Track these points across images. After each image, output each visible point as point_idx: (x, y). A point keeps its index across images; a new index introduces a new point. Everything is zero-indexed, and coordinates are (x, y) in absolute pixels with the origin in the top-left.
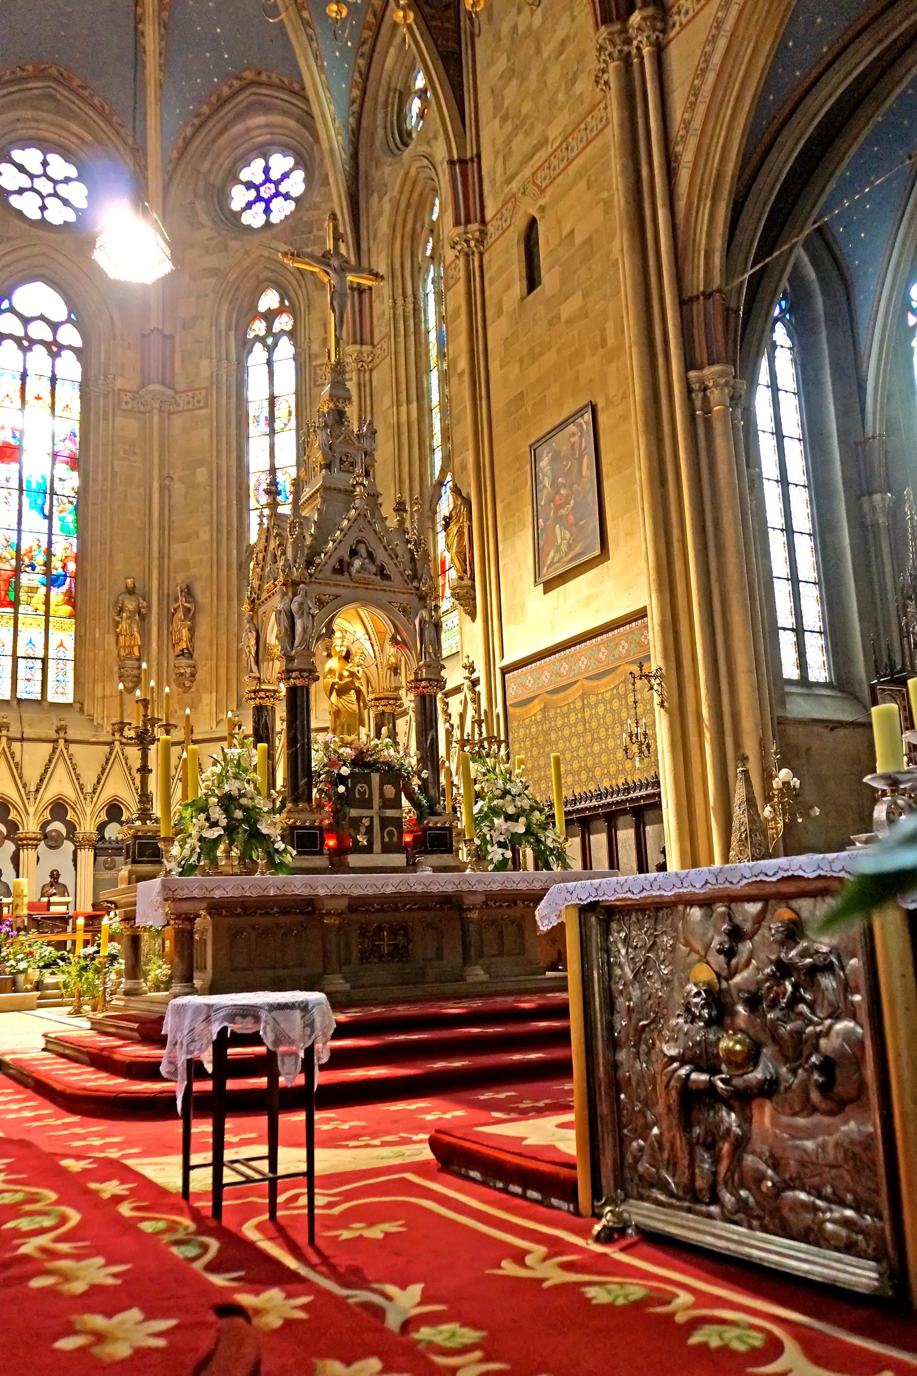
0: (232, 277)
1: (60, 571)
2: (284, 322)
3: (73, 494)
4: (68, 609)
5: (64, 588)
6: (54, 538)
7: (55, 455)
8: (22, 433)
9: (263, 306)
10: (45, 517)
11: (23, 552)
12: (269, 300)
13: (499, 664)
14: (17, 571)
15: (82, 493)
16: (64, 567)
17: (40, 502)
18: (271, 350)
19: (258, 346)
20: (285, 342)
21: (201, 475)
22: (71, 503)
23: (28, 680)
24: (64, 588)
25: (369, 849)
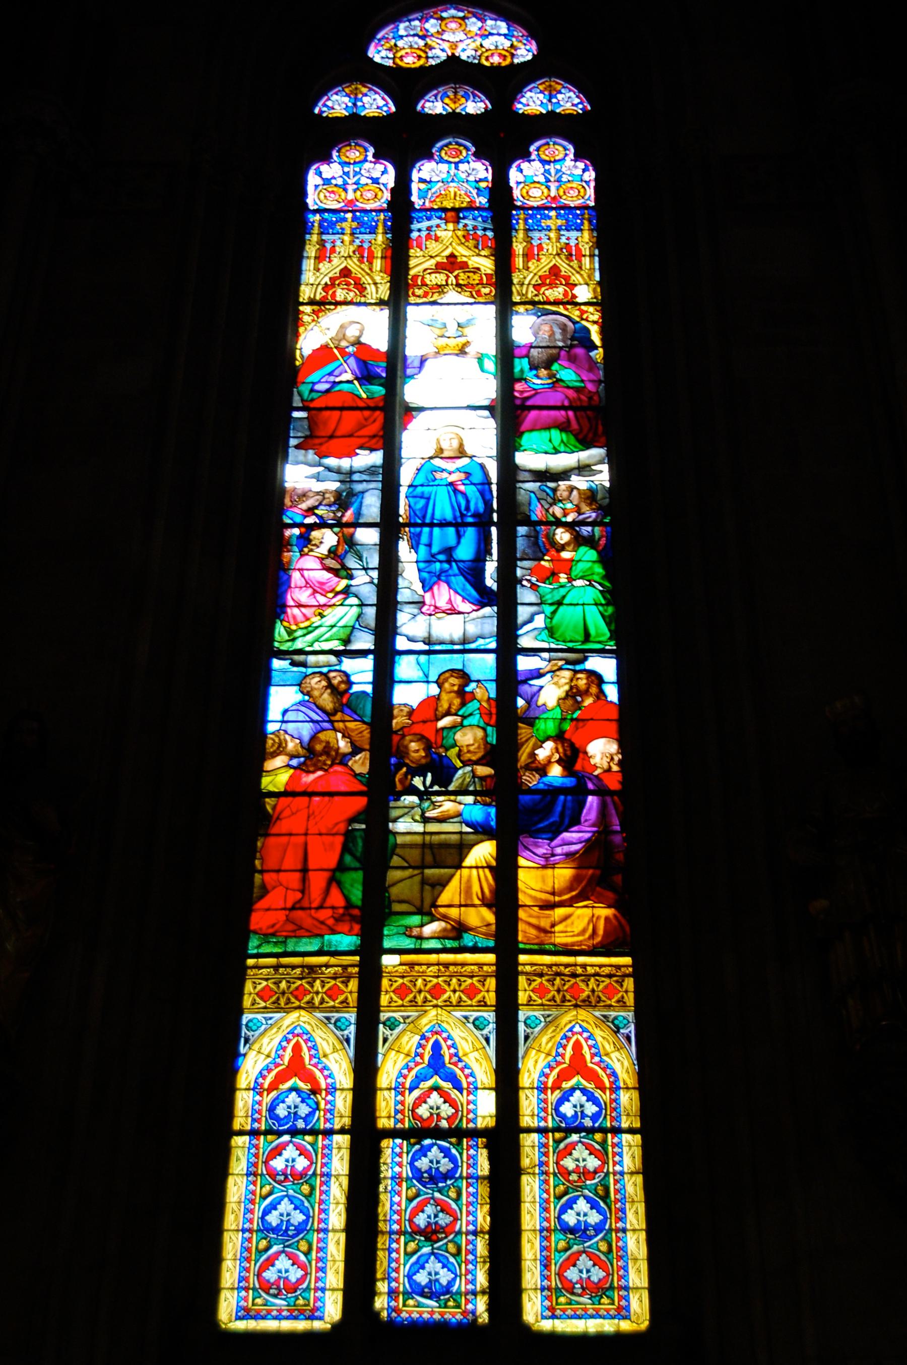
3: (590, 514)
6: (524, 663)
10: (484, 598)
11: (398, 721)
17: (465, 551)
22: (590, 542)
23: (431, 1234)
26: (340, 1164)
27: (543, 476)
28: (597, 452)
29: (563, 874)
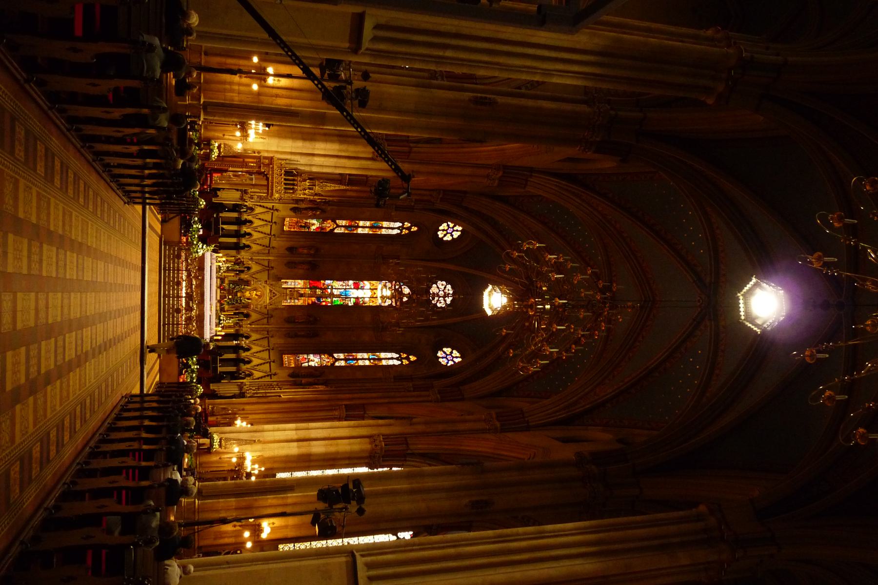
1: (322, 300)
4: (310, 302)
5: (316, 301)
7: (357, 298)
8: (364, 289)
9: (410, 357)
12: (412, 358)
13: (281, 395)
15: (347, 305)
16: (323, 302)
18: (397, 359)
19: (398, 356)
20: (400, 362)
22: (343, 303)
24: (316, 301)
25: (221, 293)
26: (292, 287)
27: (350, 300)
28: (353, 304)
29: (314, 301)
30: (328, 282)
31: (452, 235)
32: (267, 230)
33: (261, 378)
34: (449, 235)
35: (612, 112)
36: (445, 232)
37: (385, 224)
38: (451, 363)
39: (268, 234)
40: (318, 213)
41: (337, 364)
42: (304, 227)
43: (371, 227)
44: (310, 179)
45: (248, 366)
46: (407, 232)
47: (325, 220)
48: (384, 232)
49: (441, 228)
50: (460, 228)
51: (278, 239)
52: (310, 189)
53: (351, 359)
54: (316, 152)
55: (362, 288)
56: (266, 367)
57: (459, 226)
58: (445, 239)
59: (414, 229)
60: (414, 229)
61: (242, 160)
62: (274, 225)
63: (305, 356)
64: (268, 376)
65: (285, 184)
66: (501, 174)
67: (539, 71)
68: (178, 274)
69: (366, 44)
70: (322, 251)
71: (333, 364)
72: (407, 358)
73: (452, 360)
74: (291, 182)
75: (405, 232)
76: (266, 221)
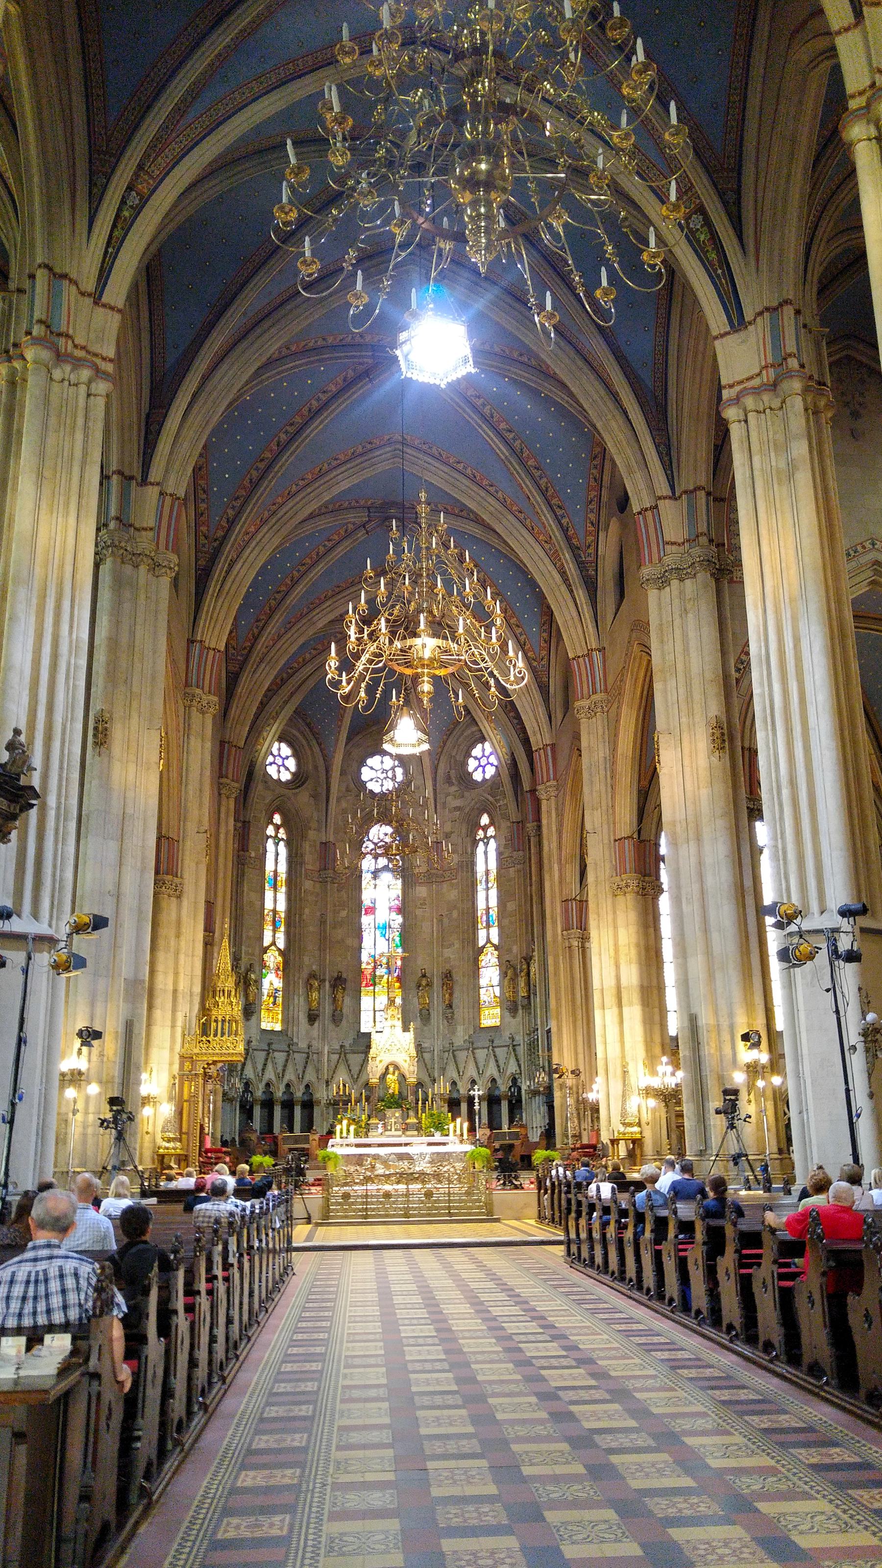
0: (467, 810)
2: (491, 831)
7: (390, 908)
12: (485, 820)
14: (375, 968)
15: (403, 926)
18: (486, 844)
20: (492, 841)
21: (455, 914)
30: (365, 957)
31: (287, 758)
32: (280, 1057)
33: (517, 1060)
34: (286, 762)
35: (112, 525)
36: (282, 769)
37: (270, 866)
38: (493, 759)
39: (288, 1055)
40: (253, 976)
41: (495, 940)
42: (275, 997)
43: (275, 888)
44: (214, 997)
45: (499, 1081)
46: (282, 831)
47: (263, 965)
48: (283, 868)
49: (275, 776)
50: (276, 745)
51: (295, 1040)
52: (229, 996)
53: (488, 918)
54: (170, 987)
55: (374, 902)
56: (501, 1053)
57: (270, 746)
58: (293, 768)
59: (277, 819)
60: (277, 819)
61: (185, 1104)
62: (273, 1047)
63: (482, 991)
64: (514, 1050)
65: (223, 1034)
66: (198, 691)
67: (73, 662)
68: (372, 1196)
69: (42, 928)
70: (314, 967)
71: (496, 948)
72: (485, 828)
73: (488, 758)
74: (220, 1024)
75: (282, 834)
76: (266, 1060)
